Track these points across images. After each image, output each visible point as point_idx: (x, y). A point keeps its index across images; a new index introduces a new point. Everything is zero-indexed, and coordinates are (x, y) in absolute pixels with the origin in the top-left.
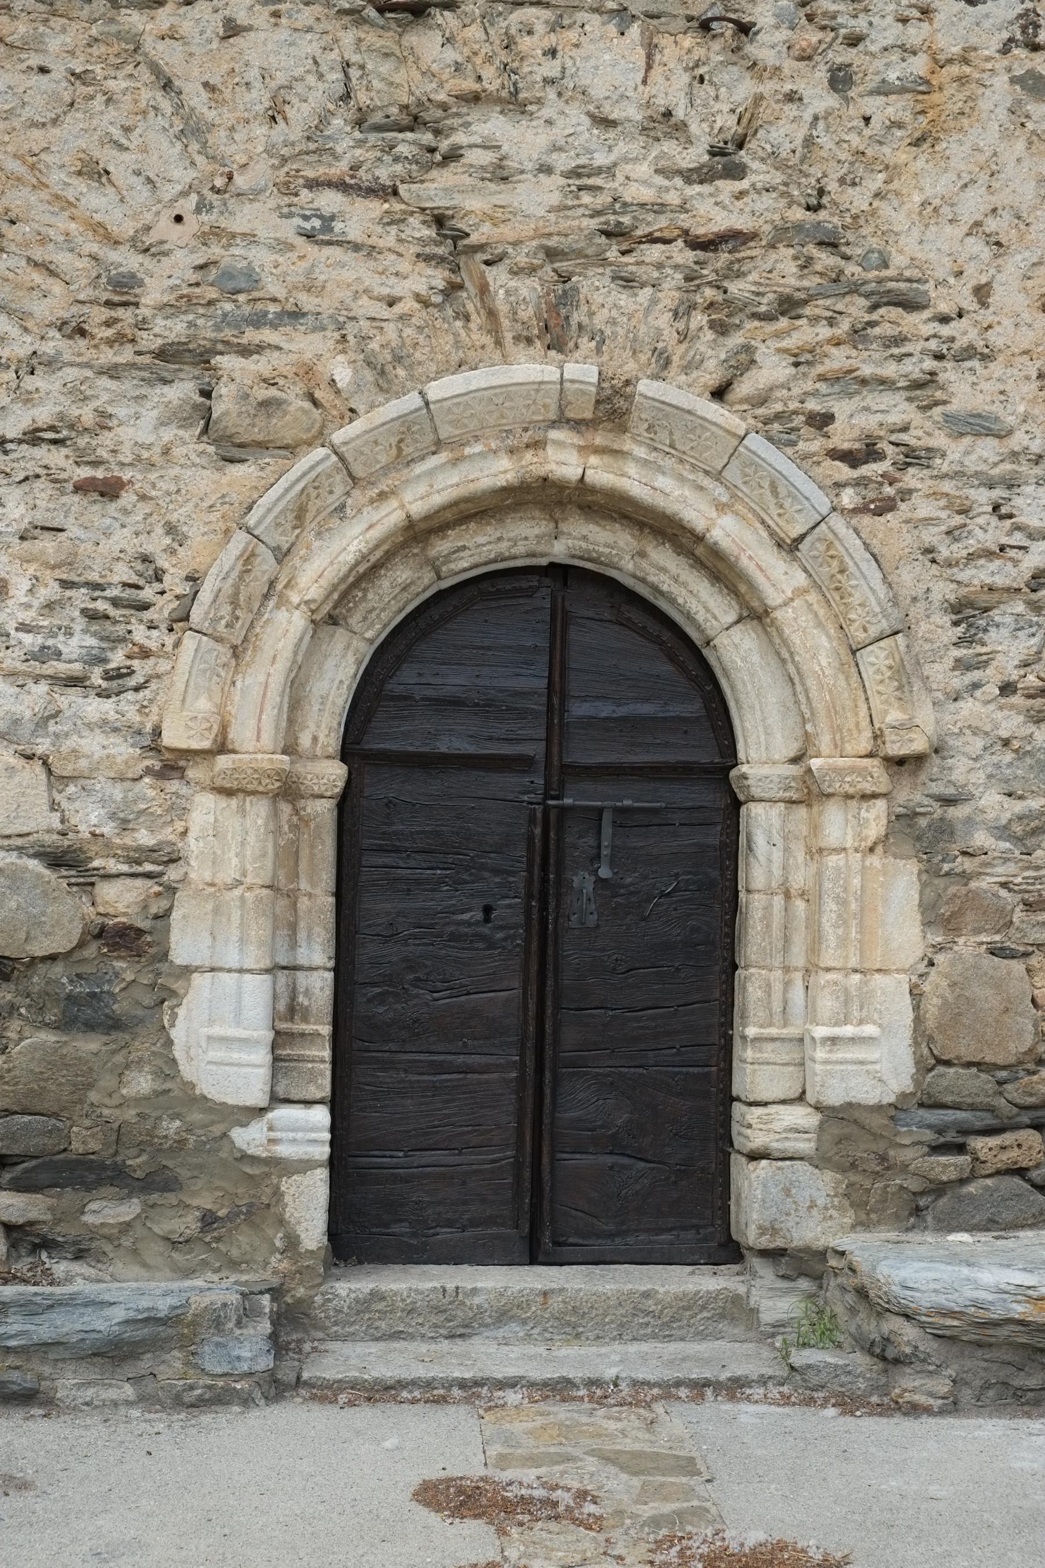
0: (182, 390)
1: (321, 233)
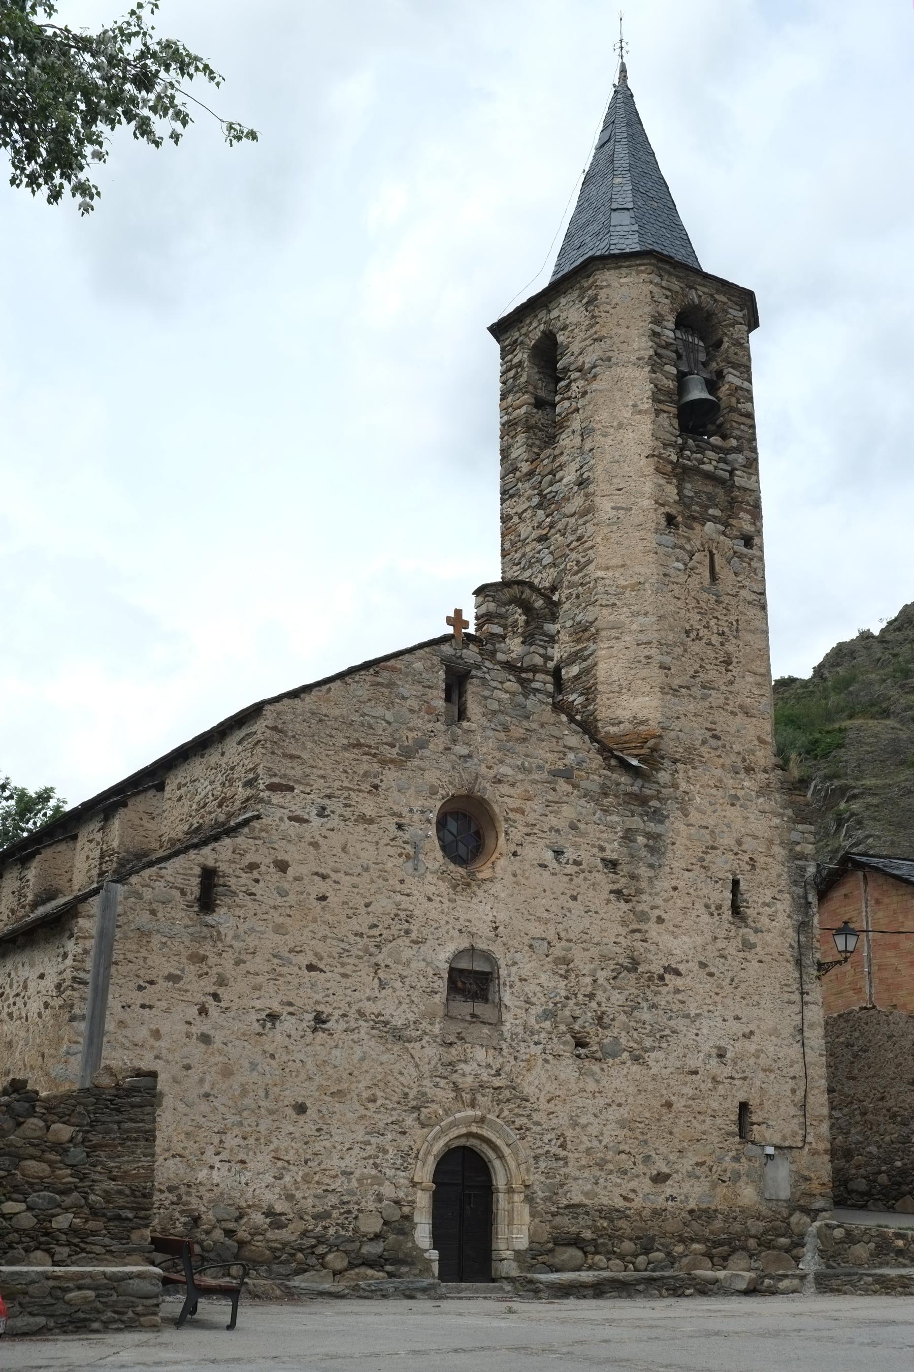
0: (415, 1115)
1: (436, 1085)
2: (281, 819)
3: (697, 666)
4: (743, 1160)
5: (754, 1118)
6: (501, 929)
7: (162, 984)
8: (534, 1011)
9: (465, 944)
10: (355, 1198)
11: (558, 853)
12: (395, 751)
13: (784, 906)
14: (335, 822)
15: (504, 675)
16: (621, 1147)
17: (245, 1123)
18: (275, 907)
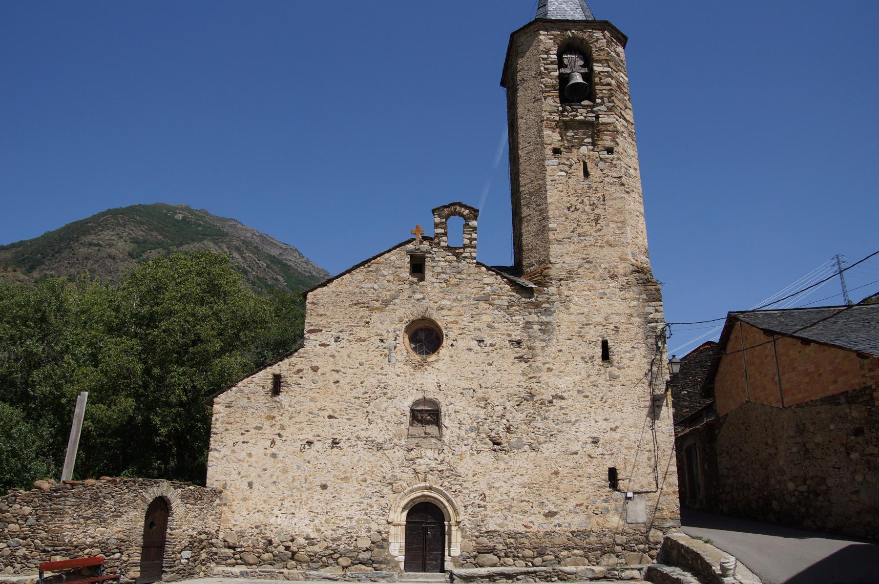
2: (315, 346)
3: (575, 226)
5: (619, 477)
7: (253, 431)
8: (464, 428)
9: (420, 396)
11: (480, 341)
13: (642, 350)
14: (344, 343)
15: (444, 253)
16: (523, 498)
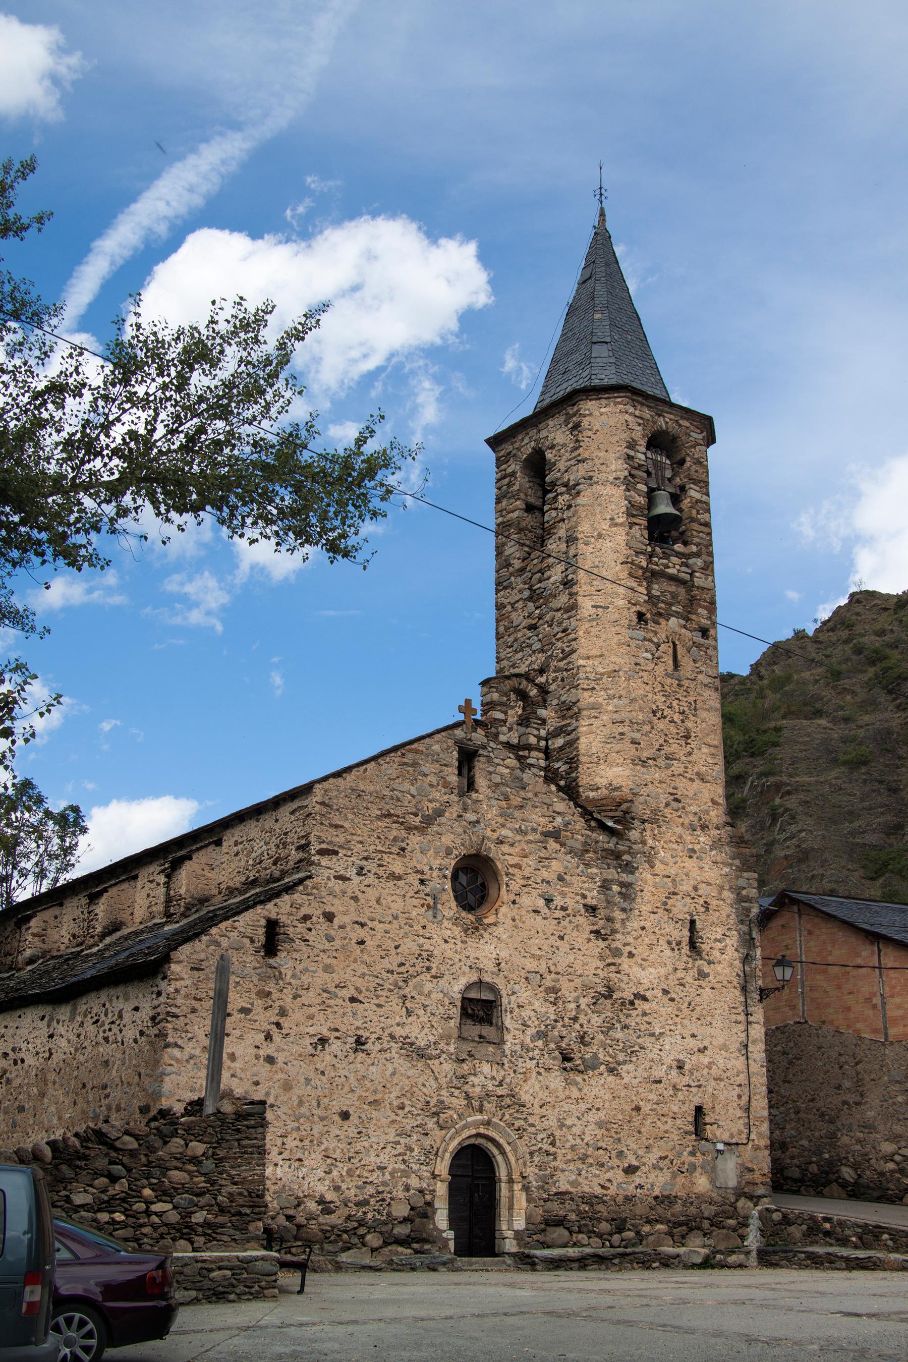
1: (452, 1095)
2: (328, 878)
3: (661, 741)
4: (698, 1154)
5: (707, 1120)
6: (503, 964)
9: (474, 978)
10: (388, 1189)
11: (549, 901)
12: (419, 819)
13: (733, 941)
14: (371, 879)
15: (505, 753)
16: (600, 1144)
17: (302, 1128)
18: (324, 951)
